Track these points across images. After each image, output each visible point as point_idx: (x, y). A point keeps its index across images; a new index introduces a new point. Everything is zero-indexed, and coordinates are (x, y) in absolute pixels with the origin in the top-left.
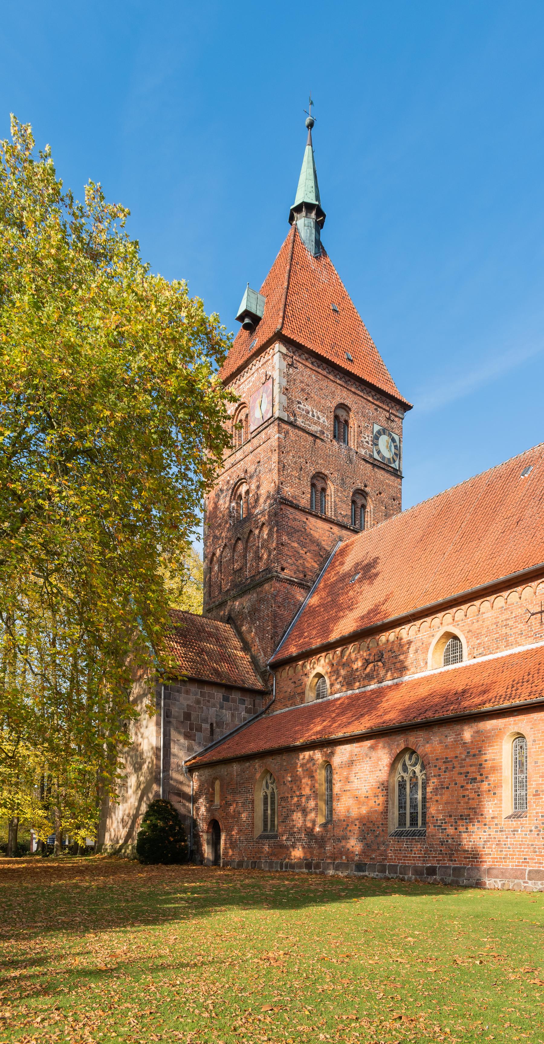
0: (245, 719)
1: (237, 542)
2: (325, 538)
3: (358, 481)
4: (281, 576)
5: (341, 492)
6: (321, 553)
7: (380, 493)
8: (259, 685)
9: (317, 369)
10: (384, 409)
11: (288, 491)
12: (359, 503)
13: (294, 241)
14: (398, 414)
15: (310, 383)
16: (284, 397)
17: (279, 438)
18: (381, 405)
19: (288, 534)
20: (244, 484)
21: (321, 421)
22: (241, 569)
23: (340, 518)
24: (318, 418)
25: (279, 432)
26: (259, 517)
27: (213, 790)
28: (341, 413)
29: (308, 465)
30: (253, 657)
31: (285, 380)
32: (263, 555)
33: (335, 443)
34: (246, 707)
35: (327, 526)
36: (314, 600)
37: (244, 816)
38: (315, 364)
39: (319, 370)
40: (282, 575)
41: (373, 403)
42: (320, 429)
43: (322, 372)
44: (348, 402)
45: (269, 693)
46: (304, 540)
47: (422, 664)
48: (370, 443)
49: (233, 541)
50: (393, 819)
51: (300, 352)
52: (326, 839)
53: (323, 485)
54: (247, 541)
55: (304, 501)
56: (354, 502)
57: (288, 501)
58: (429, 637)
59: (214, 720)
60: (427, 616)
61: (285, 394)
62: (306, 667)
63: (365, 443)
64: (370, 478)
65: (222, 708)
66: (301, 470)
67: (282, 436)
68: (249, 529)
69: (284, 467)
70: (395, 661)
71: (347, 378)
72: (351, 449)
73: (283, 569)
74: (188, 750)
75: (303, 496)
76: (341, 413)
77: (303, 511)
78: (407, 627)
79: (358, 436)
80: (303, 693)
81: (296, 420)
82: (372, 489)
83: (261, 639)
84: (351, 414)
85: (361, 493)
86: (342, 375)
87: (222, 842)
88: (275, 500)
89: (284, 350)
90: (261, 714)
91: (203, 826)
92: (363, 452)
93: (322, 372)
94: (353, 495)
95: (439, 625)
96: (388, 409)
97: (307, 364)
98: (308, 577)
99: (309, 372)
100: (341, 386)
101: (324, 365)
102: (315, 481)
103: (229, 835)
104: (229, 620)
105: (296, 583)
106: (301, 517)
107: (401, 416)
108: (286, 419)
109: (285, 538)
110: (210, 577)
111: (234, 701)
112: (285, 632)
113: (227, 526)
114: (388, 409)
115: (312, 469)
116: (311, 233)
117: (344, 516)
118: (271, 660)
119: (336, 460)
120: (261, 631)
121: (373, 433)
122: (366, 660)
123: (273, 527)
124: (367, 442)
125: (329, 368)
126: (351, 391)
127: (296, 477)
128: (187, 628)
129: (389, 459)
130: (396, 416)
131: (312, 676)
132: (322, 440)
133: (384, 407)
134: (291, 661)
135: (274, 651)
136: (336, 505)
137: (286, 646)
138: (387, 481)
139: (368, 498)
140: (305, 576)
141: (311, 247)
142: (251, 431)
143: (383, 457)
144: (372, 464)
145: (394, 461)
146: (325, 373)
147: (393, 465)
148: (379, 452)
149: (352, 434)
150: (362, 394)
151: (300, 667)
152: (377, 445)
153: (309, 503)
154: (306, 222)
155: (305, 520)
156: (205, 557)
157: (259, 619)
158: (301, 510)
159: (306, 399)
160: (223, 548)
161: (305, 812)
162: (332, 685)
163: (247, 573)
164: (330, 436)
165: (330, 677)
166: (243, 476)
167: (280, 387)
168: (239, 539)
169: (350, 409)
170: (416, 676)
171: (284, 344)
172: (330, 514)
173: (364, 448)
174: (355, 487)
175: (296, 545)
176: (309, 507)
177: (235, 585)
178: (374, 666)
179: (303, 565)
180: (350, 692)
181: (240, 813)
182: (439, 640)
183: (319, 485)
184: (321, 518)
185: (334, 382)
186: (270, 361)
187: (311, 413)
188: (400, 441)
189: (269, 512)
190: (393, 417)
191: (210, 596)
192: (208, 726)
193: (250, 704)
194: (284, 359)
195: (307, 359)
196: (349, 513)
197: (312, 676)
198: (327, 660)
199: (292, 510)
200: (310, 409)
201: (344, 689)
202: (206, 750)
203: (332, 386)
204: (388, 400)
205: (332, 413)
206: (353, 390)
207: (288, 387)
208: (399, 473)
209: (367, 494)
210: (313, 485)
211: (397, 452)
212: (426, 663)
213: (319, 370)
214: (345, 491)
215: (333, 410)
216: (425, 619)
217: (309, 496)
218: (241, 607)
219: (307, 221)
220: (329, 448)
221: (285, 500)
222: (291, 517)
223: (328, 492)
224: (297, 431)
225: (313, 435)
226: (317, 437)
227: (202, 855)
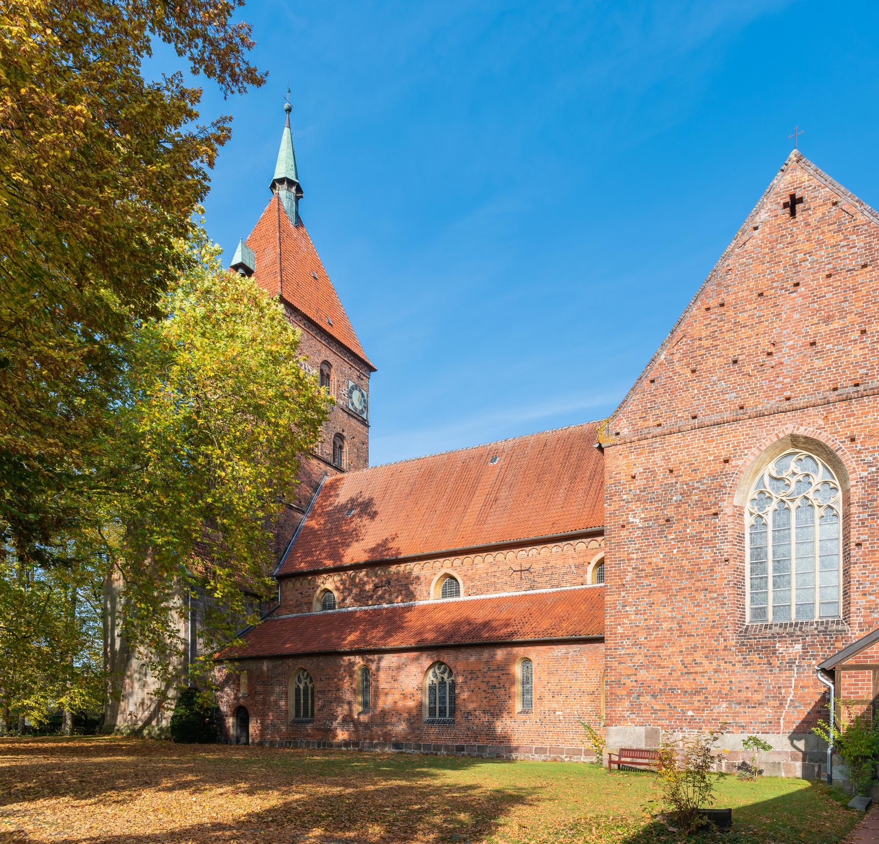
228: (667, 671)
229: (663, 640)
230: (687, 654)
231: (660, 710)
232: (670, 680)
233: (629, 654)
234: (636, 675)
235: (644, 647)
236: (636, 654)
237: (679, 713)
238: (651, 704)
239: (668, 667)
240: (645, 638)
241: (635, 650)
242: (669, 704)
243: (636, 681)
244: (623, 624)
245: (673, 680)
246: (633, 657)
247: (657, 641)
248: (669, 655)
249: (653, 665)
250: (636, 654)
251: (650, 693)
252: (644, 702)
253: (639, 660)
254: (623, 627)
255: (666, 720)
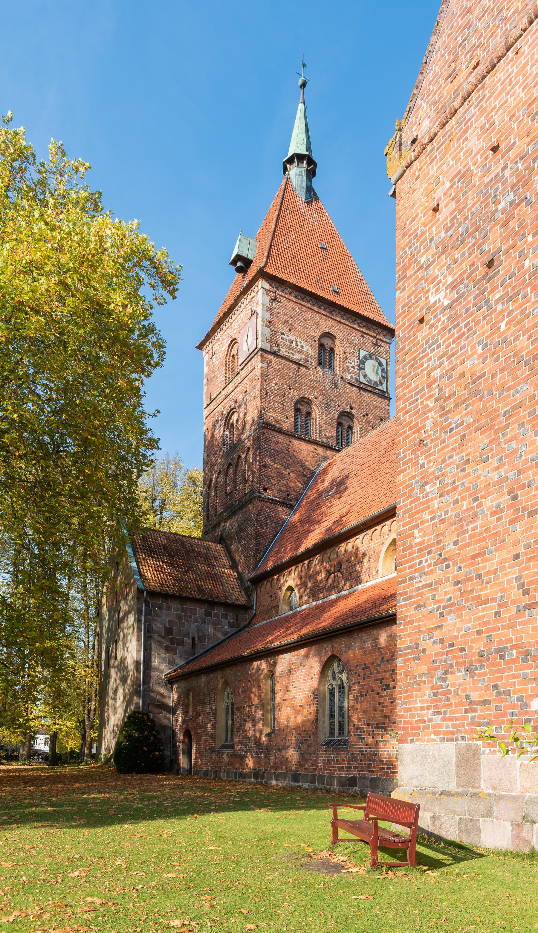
0: (227, 633)
1: (228, 467)
2: (309, 459)
3: (344, 404)
4: (263, 496)
5: (326, 415)
6: (305, 473)
7: (367, 415)
8: (242, 600)
9: (301, 302)
10: (371, 336)
11: (271, 416)
12: (346, 424)
13: (285, 189)
14: (385, 340)
15: (294, 315)
16: (268, 329)
17: (261, 367)
18: (367, 332)
19: (271, 456)
20: (236, 413)
21: (305, 350)
22: (231, 492)
23: (325, 440)
24: (302, 347)
25: (262, 362)
26: (246, 441)
27: (189, 701)
28: (327, 342)
29: (292, 391)
30: (239, 573)
31: (268, 313)
32: (249, 477)
33: (319, 369)
34: (229, 622)
35: (311, 447)
36: (295, 518)
37: (209, 725)
38: (299, 297)
39: (303, 303)
40: (264, 495)
41: (359, 331)
42: (304, 357)
43: (306, 304)
44: (333, 331)
45: (251, 607)
46: (287, 462)
47: (374, 572)
48: (356, 367)
49: (226, 467)
50: (323, 728)
51: (283, 287)
52: (270, 749)
53: (308, 409)
54: (237, 466)
55: (288, 425)
56: (339, 424)
57: (271, 425)
58: (380, 545)
59: (196, 634)
60: (378, 524)
61: (268, 327)
62: (280, 580)
63: (350, 368)
64: (356, 401)
65: (204, 622)
66: (284, 395)
67: (265, 365)
68: (237, 454)
69: (267, 393)
70: (351, 570)
71: (332, 309)
72: (336, 375)
73: (265, 490)
74: (169, 664)
75: (286, 420)
76: (327, 342)
77: (286, 434)
78: (361, 536)
79: (344, 361)
80: (278, 606)
81: (279, 350)
82: (358, 410)
83: (246, 557)
84: (337, 342)
85: (347, 415)
86: (326, 306)
87: (194, 752)
88: (258, 426)
89: (267, 286)
90: (243, 628)
91: (180, 736)
92: (348, 376)
93: (306, 304)
94: (339, 417)
95: (388, 532)
96: (374, 335)
97: (291, 298)
98: (291, 496)
99: (292, 305)
100: (326, 316)
101: (308, 298)
102: (299, 406)
103: (198, 745)
104: (221, 540)
105: (279, 502)
106: (281, 439)
107: (388, 341)
108: (269, 349)
109: (267, 460)
110: (208, 502)
111: (216, 616)
112: (267, 549)
113: (221, 453)
114: (374, 335)
115: (296, 395)
116: (302, 181)
117: (329, 438)
118: (252, 575)
119: (320, 386)
120: (246, 548)
121: (359, 358)
122: (328, 571)
123: (256, 451)
124: (353, 367)
125: (313, 300)
126: (335, 320)
127: (279, 403)
128: (176, 549)
129: (376, 382)
130: (383, 341)
131: (284, 588)
132: (306, 367)
133: (371, 333)
134: (267, 576)
135: (256, 566)
136: (320, 427)
137: (265, 563)
138: (374, 403)
139: (355, 420)
140: (288, 495)
141: (302, 193)
142: (240, 363)
143: (370, 381)
144: (358, 387)
145: (381, 384)
146: (309, 305)
147: (380, 388)
148: (365, 376)
149: (338, 360)
150: (347, 323)
151: (275, 582)
152: (363, 369)
153: (292, 427)
154: (298, 171)
155: (288, 443)
156: (204, 484)
157: (244, 538)
158: (284, 433)
159: (290, 330)
160: (219, 474)
161: (254, 722)
162: (301, 597)
163: (237, 496)
164: (314, 363)
165: (299, 590)
166: (233, 406)
167: (263, 320)
168: (230, 464)
169: (335, 337)
170: (369, 584)
171: (266, 281)
172: (315, 436)
173: (349, 373)
174: (340, 410)
175: (279, 466)
176: (293, 431)
177: (226, 508)
178: (334, 577)
179: (286, 485)
180: (315, 603)
181: (206, 724)
182: (388, 548)
183: (304, 409)
184: (304, 440)
185: (319, 313)
186: (255, 298)
187: (294, 343)
188: (387, 364)
189: (253, 437)
190: (379, 343)
191: (208, 519)
192: (190, 641)
193: (233, 618)
194: (267, 294)
195: (290, 293)
196: (335, 434)
197: (284, 588)
198: (297, 573)
199: (275, 434)
200: (293, 339)
201: (311, 600)
202: (187, 663)
203: (317, 317)
204: (374, 327)
205: (317, 342)
206: (338, 319)
207: (271, 320)
208: (386, 395)
209: (353, 415)
210: (297, 410)
211: (385, 375)
212: (378, 571)
213: (303, 303)
214: (330, 414)
215: (317, 339)
216: (376, 528)
217: (293, 420)
218: (230, 527)
219: (298, 170)
220: (313, 374)
221: (268, 424)
222: (274, 440)
223: (313, 416)
224: (280, 360)
225: (296, 363)
226: (300, 365)
227: (179, 764)
228: (492, 608)
229: (484, 539)
230: (529, 560)
231: (480, 703)
232: (497, 628)
233: (429, 585)
234: (440, 627)
235: (455, 563)
236: (439, 582)
237: (514, 706)
238: (464, 690)
239: (494, 600)
240: (456, 543)
241: (439, 573)
242: (495, 687)
243: (442, 641)
244: (423, 522)
245: (504, 627)
246: (436, 589)
247: (476, 542)
248: (495, 572)
249: (467, 600)
250: (439, 582)
251: (463, 663)
252: (454, 685)
253: (446, 593)
254: (422, 530)
255: (492, 723)
